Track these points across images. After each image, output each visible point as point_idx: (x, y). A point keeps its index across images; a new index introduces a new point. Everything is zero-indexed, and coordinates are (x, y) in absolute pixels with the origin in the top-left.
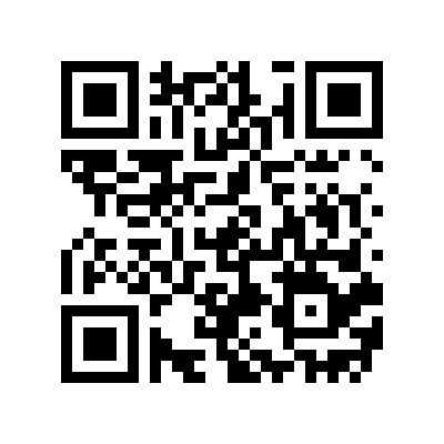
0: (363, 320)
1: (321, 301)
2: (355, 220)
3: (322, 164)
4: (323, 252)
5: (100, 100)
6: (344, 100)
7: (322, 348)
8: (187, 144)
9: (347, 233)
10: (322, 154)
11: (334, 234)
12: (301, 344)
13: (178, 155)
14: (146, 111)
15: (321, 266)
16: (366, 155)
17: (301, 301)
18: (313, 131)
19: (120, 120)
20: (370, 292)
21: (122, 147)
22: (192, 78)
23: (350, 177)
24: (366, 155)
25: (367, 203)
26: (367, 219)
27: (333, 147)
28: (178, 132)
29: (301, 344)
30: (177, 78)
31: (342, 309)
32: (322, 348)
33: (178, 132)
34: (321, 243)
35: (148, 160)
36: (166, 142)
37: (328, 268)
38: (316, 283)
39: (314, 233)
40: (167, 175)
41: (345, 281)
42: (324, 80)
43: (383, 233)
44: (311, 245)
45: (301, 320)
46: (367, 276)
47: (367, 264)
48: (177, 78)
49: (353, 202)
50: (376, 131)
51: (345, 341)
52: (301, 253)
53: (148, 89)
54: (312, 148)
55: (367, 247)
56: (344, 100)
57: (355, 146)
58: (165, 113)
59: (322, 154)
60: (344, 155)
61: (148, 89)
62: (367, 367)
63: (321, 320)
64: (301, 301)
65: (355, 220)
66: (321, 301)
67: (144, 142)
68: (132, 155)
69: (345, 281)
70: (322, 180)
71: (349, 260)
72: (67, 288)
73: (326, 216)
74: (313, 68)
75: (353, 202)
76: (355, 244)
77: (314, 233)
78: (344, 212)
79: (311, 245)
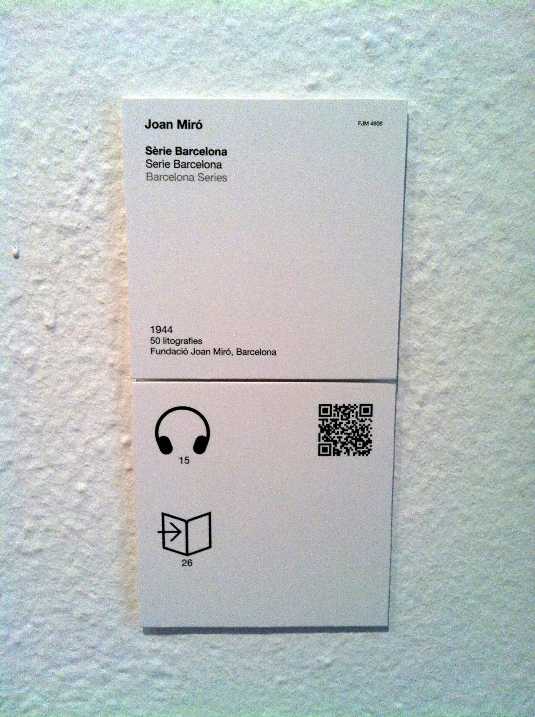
0: (368, 446)
1: (361, 443)
2: (367, 430)
3: (362, 421)
4: (362, 435)
5: (325, 411)
6: (366, 410)
7: (361, 450)
8: (340, 418)
9: (366, 432)
10: (362, 419)
11: (364, 432)
12: (358, 450)
13: (338, 419)
14: (333, 412)
15: (362, 437)
16: (369, 419)
17: (358, 443)
18: (361, 415)
19: (329, 414)
20: (370, 441)
21: (329, 418)
22: (341, 407)
23: (367, 423)
24: (369, 419)
25: (369, 427)
26: (369, 430)
27: (364, 418)
28: (338, 416)
29: (358, 450)
30: (338, 407)
31: (365, 444)
32: (361, 450)
33: (338, 416)
34: (362, 434)
35: (333, 420)
36: (336, 417)
37: (363, 438)
38: (361, 440)
39: (360, 432)
40: (336, 423)
41: (365, 440)
42: (363, 407)
43: (372, 432)
44: (360, 433)
45: (358, 446)
46: (369, 439)
47: (369, 437)
48: (338, 407)
49: (367, 427)
50: (371, 415)
51: (365, 449)
52: (358, 435)
53: (333, 409)
55: (369, 434)
56: (366, 410)
57: (368, 418)
58: (336, 413)
59: (362, 419)
60: (366, 419)
61: (333, 409)
62: (369, 453)
63: (361, 446)
64: (358, 443)
65: (367, 430)
66: (361, 443)
67: (333, 417)
68: (331, 419)
69: (365, 440)
70: (362, 423)
71: (366, 436)
72: (319, 441)
73: (362, 429)
74: (361, 405)
75: (367, 427)
76: (367, 434)
77: (360, 432)
78: (366, 429)
79: (360, 433)
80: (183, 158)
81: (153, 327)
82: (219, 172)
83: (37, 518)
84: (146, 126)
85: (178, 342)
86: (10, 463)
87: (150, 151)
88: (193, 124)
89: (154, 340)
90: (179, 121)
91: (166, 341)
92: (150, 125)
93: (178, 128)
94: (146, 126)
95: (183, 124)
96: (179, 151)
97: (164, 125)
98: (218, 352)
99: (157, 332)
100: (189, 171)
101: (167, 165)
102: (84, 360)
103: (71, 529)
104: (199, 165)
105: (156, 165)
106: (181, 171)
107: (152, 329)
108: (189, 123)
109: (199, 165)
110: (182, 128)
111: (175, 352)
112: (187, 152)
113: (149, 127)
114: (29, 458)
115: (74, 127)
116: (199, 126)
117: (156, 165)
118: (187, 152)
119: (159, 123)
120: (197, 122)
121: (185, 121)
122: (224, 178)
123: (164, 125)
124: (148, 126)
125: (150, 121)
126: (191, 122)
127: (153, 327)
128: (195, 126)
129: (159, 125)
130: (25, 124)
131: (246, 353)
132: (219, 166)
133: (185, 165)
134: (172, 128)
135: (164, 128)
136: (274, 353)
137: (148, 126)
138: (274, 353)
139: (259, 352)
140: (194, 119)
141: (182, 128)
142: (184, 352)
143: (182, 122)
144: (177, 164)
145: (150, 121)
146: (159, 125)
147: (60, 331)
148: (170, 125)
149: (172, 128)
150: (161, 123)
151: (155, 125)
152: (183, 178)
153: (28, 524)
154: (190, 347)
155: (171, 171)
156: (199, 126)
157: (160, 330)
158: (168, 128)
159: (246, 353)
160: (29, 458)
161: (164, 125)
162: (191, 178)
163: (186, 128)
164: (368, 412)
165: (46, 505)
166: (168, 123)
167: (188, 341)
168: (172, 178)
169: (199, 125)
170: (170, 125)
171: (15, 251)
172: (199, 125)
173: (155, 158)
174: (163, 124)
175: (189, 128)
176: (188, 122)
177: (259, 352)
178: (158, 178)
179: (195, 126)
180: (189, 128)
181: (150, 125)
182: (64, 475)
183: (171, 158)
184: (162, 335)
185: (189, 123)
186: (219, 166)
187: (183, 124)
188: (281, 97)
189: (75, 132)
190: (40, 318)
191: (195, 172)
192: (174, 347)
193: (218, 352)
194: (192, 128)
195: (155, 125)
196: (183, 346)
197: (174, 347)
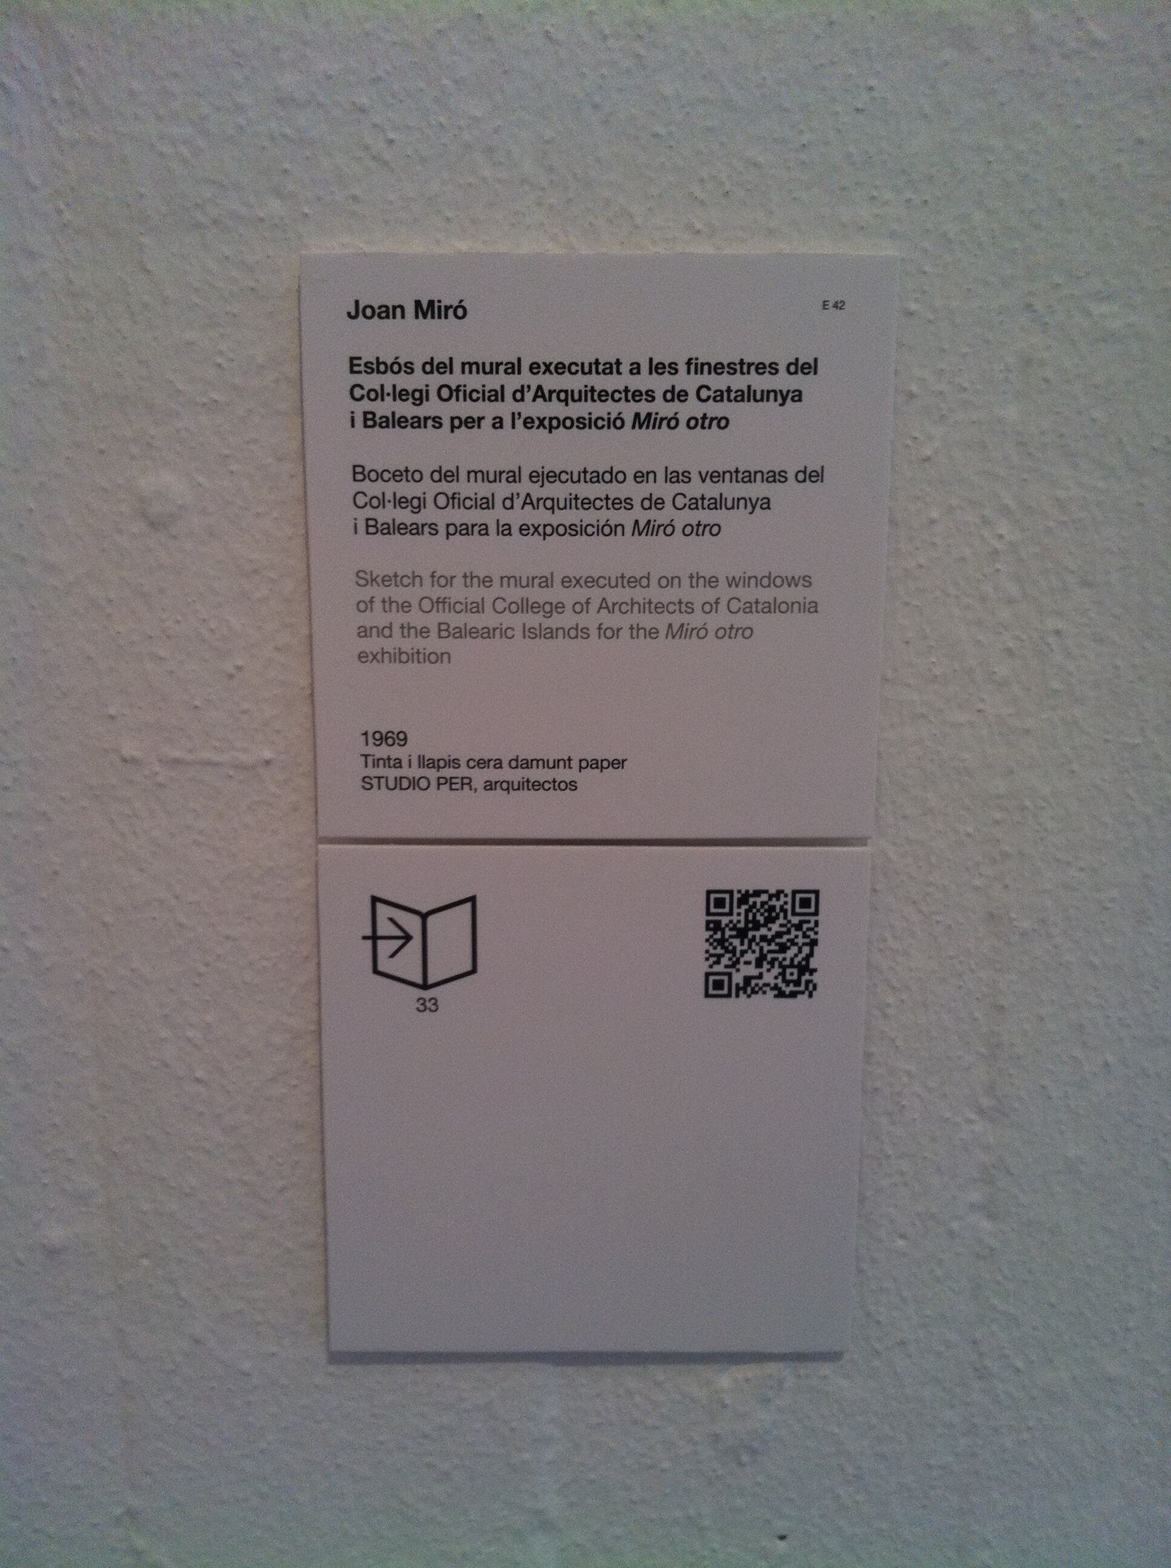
6: (805, 903)
18: (794, 914)
42: (798, 896)
54: (795, 920)
56: (805, 903)
74: (794, 892)
81: (366, 734)
84: (349, 314)
88: (447, 308)
90: (418, 304)
92: (358, 312)
93: (417, 317)
94: (349, 314)
95: (427, 310)
97: (387, 311)
99: (374, 744)
107: (364, 736)
108: (439, 307)
110: (425, 317)
113: (356, 317)
116: (460, 312)
119: (376, 307)
120: (455, 304)
121: (431, 303)
123: (387, 312)
124: (353, 313)
125: (357, 302)
126: (443, 304)
127: (366, 734)
128: (451, 312)
129: (377, 311)
134: (403, 317)
135: (387, 317)
137: (353, 313)
141: (425, 317)
145: (357, 302)
146: (377, 311)
148: (398, 311)
149: (403, 317)
150: (380, 307)
151: (369, 312)
156: (460, 312)
158: (394, 317)
161: (387, 312)
163: (433, 317)
164: (809, 907)
166: (394, 308)
169: (460, 311)
170: (398, 311)
172: (460, 311)
174: (384, 309)
175: (440, 317)
176: (436, 304)
179: (451, 312)
180: (440, 317)
181: (358, 312)
185: (439, 307)
187: (427, 310)
194: (446, 317)
195: (369, 312)
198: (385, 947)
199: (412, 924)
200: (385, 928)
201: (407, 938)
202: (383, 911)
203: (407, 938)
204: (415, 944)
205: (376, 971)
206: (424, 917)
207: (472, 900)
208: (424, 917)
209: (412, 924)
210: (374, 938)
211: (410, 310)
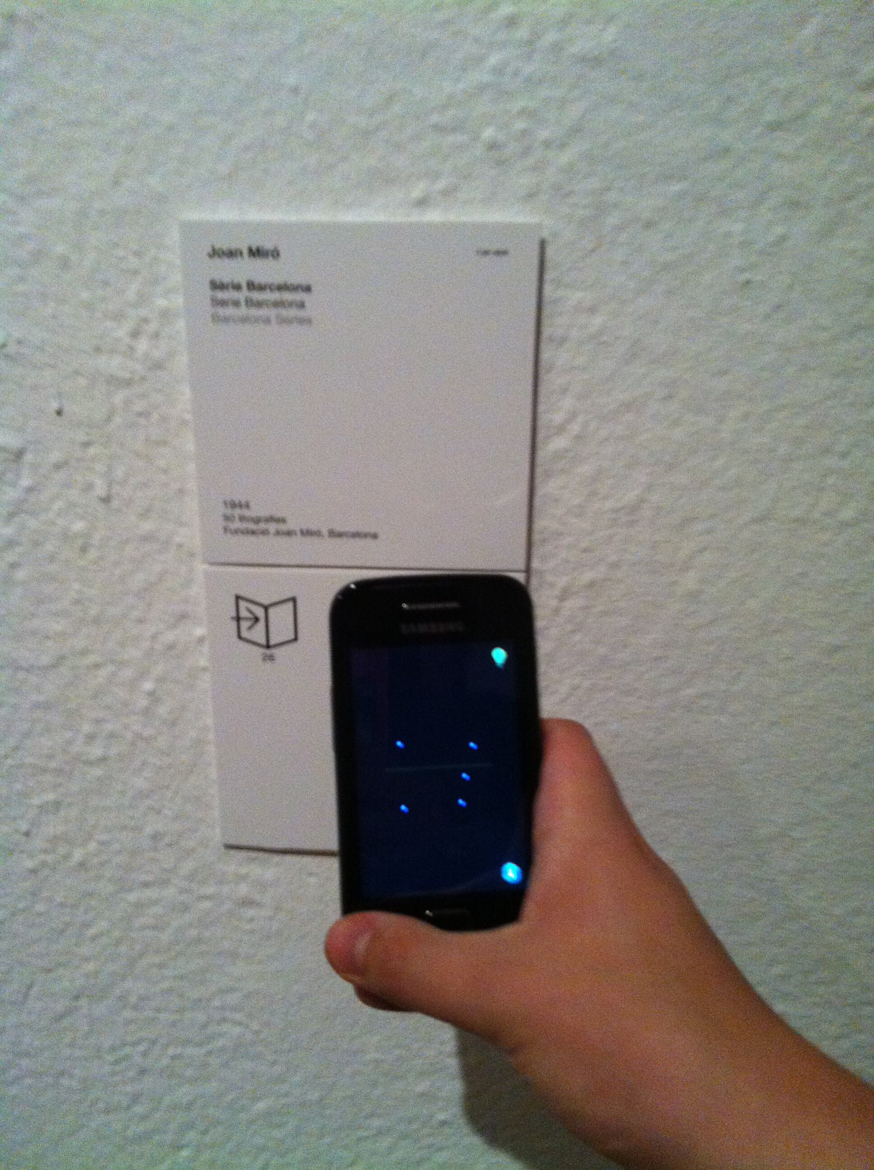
80: (257, 296)
82: (301, 313)
83: (98, 721)
85: (257, 521)
86: (63, 658)
87: (216, 286)
89: (227, 518)
91: (242, 519)
92: (215, 253)
95: (256, 253)
96: (251, 286)
98: (307, 533)
100: (263, 312)
101: (236, 304)
102: (146, 538)
103: (138, 736)
104: (277, 304)
105: (223, 303)
106: (254, 312)
109: (277, 304)
111: (253, 533)
112: (261, 288)
114: (84, 652)
115: (121, 253)
117: (223, 303)
118: (261, 288)
121: (258, 250)
122: (307, 321)
123: (232, 254)
130: (60, 249)
131: (340, 535)
132: (302, 305)
133: (259, 304)
136: (375, 536)
138: (375, 536)
139: (356, 535)
140: (268, 246)
142: (265, 532)
143: (254, 248)
144: (249, 303)
147: (115, 503)
152: (257, 320)
153: (87, 728)
154: (272, 527)
155: (243, 311)
157: (234, 505)
159: (340, 535)
160: (84, 652)
161: (232, 254)
162: (267, 321)
165: (108, 707)
167: (271, 519)
168: (245, 320)
171: (55, 405)
173: (221, 295)
177: (356, 535)
178: (226, 320)
181: (215, 253)
182: (128, 673)
183: (242, 295)
184: (237, 512)
186: (302, 305)
187: (256, 253)
188: (380, 217)
189: (121, 259)
190: (89, 487)
191: (272, 313)
192: (252, 526)
193: (307, 533)
196: (262, 526)
197: (252, 526)
198: (245, 625)
199: (260, 612)
200: (244, 613)
201: (257, 619)
202: (243, 604)
203: (257, 619)
204: (261, 624)
205: (240, 637)
206: (266, 608)
207: (294, 600)
208: (266, 608)
209: (260, 612)
210: (238, 619)
211: (245, 252)
